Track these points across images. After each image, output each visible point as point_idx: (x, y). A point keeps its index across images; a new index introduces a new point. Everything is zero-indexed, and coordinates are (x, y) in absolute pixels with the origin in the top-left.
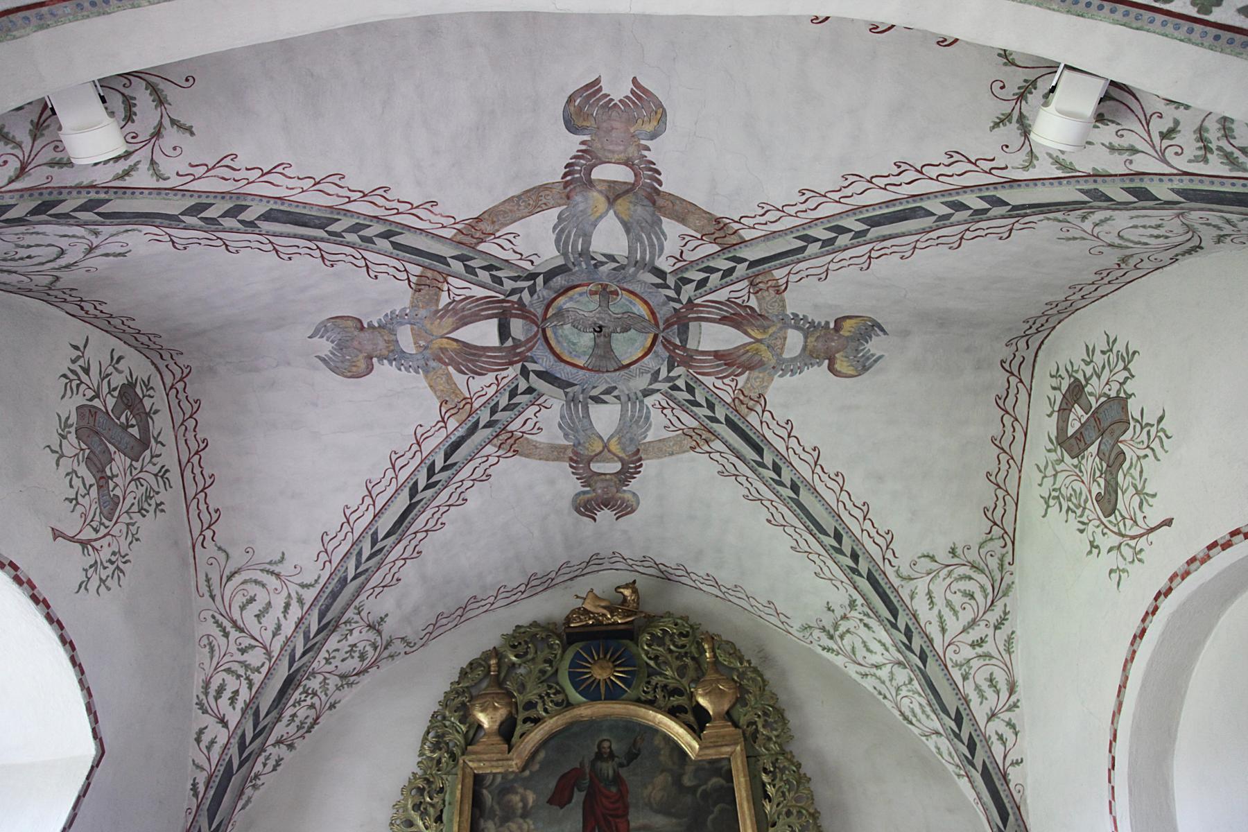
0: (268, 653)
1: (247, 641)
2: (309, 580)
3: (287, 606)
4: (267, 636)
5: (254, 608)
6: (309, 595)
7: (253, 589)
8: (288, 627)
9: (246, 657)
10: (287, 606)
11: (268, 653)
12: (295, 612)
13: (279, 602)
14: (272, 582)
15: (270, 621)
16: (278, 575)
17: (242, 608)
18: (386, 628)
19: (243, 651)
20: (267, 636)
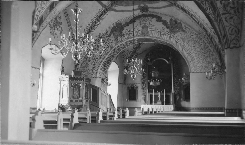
0: (128, 57)
1: (126, 57)
2: (131, 51)
3: (129, 54)
4: (128, 56)
5: (126, 54)
6: (131, 52)
7: (126, 53)
8: (130, 55)
9: (127, 58)
10: (129, 54)
11: (128, 57)
12: (130, 54)
13: (129, 53)
14: (128, 52)
15: (128, 55)
16: (128, 51)
17: (126, 54)
18: (139, 53)
19: (126, 57)
20: (128, 56)
